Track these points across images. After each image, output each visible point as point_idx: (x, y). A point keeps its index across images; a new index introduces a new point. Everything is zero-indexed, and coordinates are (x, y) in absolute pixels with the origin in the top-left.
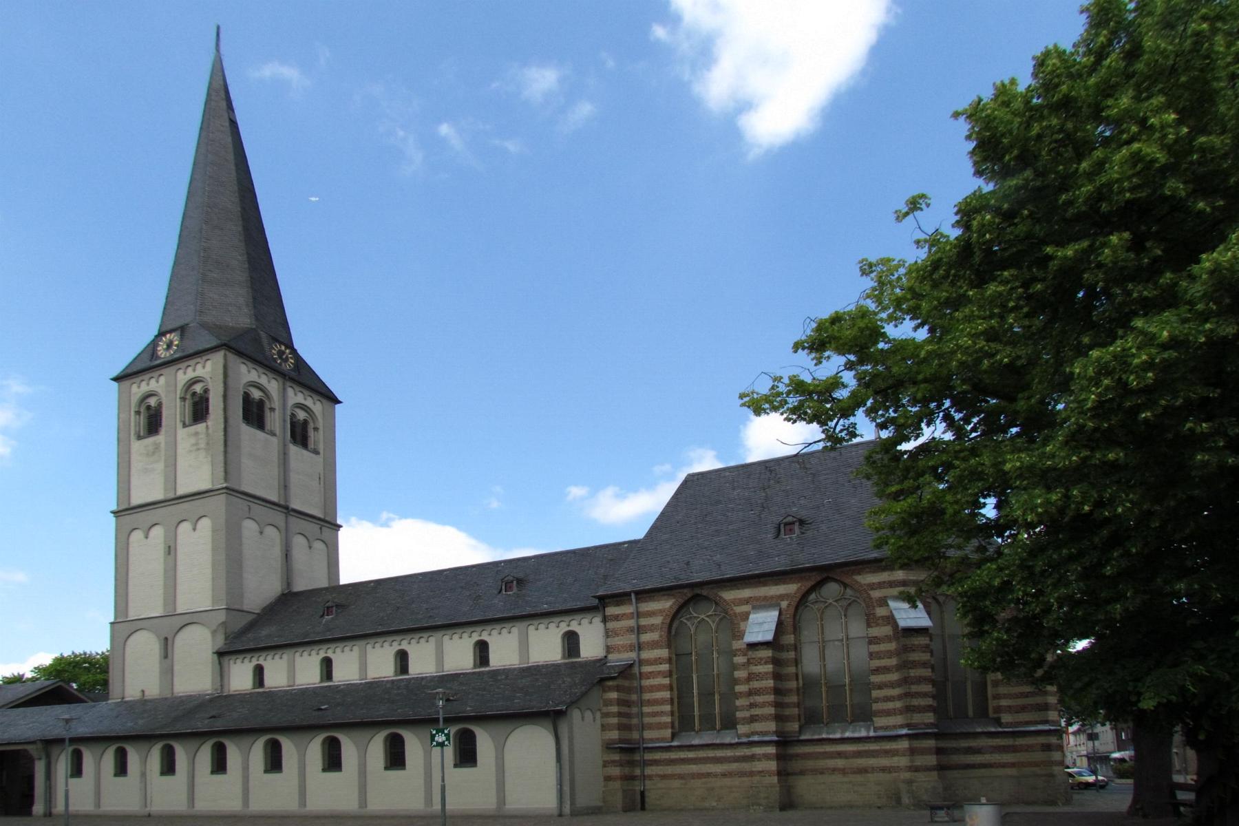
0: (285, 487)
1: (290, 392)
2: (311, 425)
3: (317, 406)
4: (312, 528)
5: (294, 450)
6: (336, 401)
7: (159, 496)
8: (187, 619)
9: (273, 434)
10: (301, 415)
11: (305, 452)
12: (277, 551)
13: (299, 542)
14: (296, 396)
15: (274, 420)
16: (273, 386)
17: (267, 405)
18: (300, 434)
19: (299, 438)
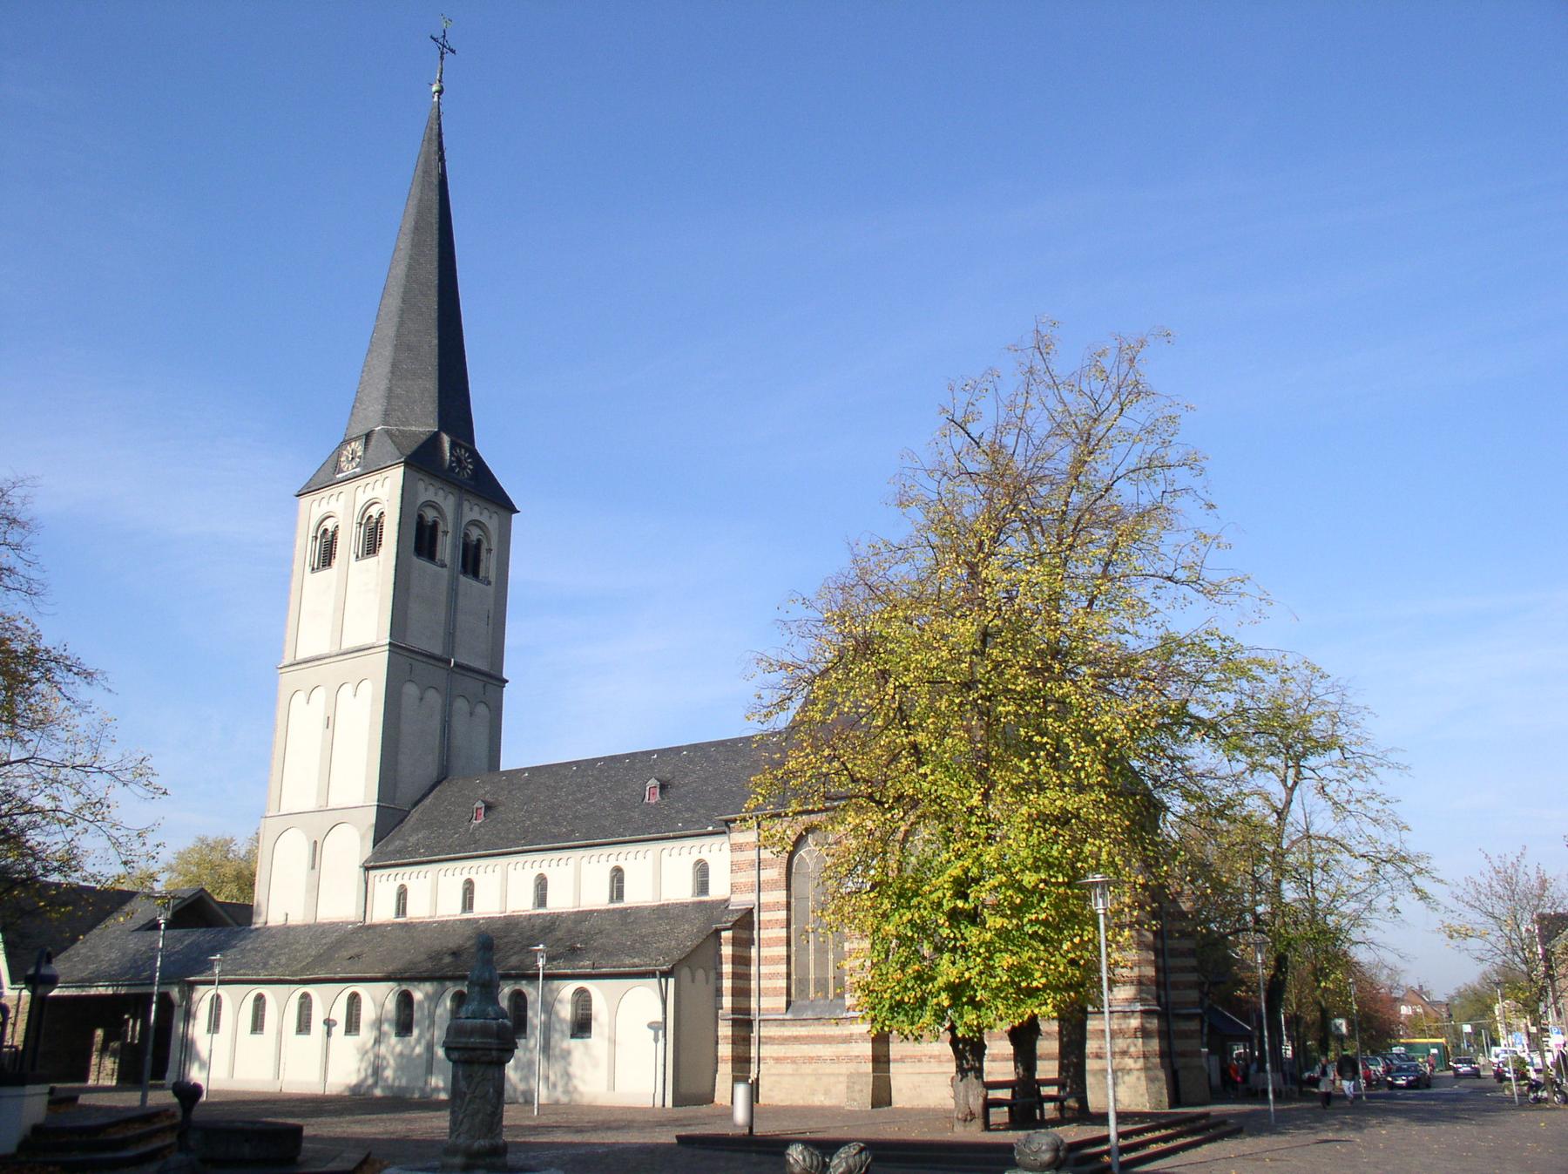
0: (451, 635)
1: (466, 506)
2: (484, 546)
3: (490, 520)
4: (473, 685)
5: (465, 581)
6: (512, 510)
7: (325, 650)
8: (337, 816)
9: (443, 566)
10: (475, 534)
11: (474, 583)
12: (436, 723)
13: (461, 705)
14: (473, 512)
15: (446, 547)
16: (447, 502)
17: (441, 527)
18: (471, 559)
19: (470, 567)
